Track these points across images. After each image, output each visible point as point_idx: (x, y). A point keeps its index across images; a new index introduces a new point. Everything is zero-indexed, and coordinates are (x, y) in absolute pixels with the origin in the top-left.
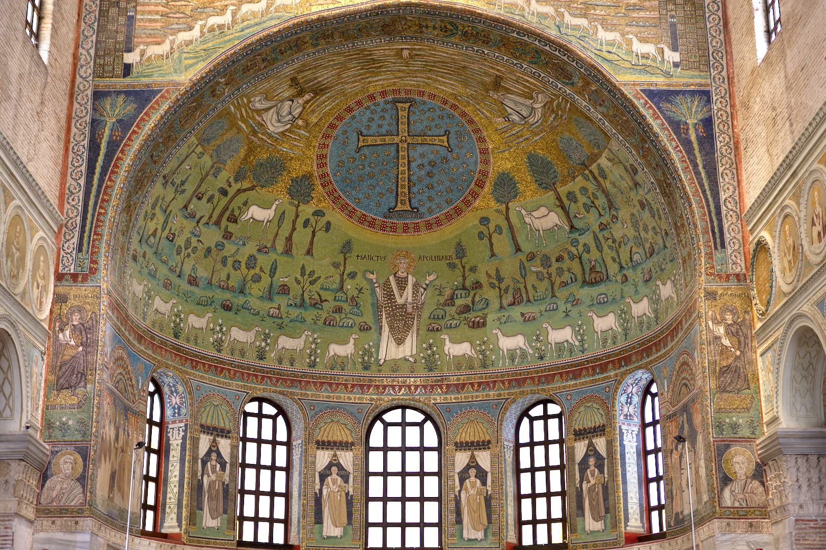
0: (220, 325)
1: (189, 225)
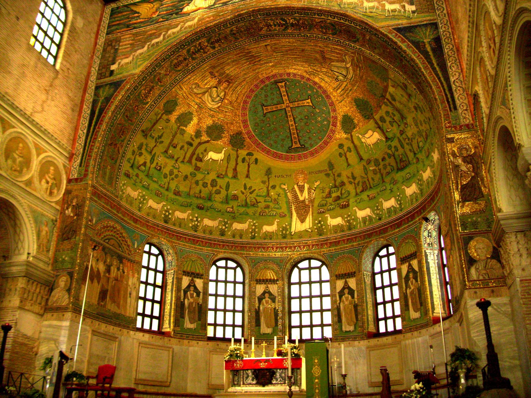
0: (197, 217)
1: (171, 163)
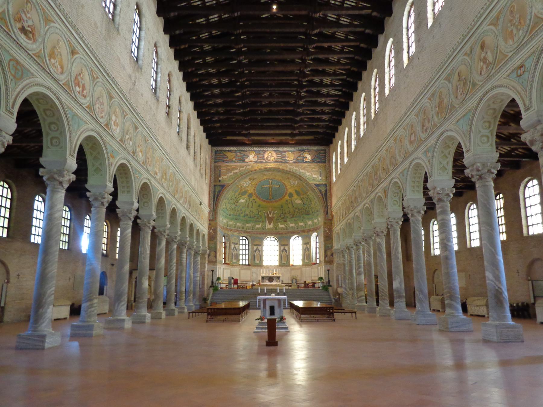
1: (229, 205)
